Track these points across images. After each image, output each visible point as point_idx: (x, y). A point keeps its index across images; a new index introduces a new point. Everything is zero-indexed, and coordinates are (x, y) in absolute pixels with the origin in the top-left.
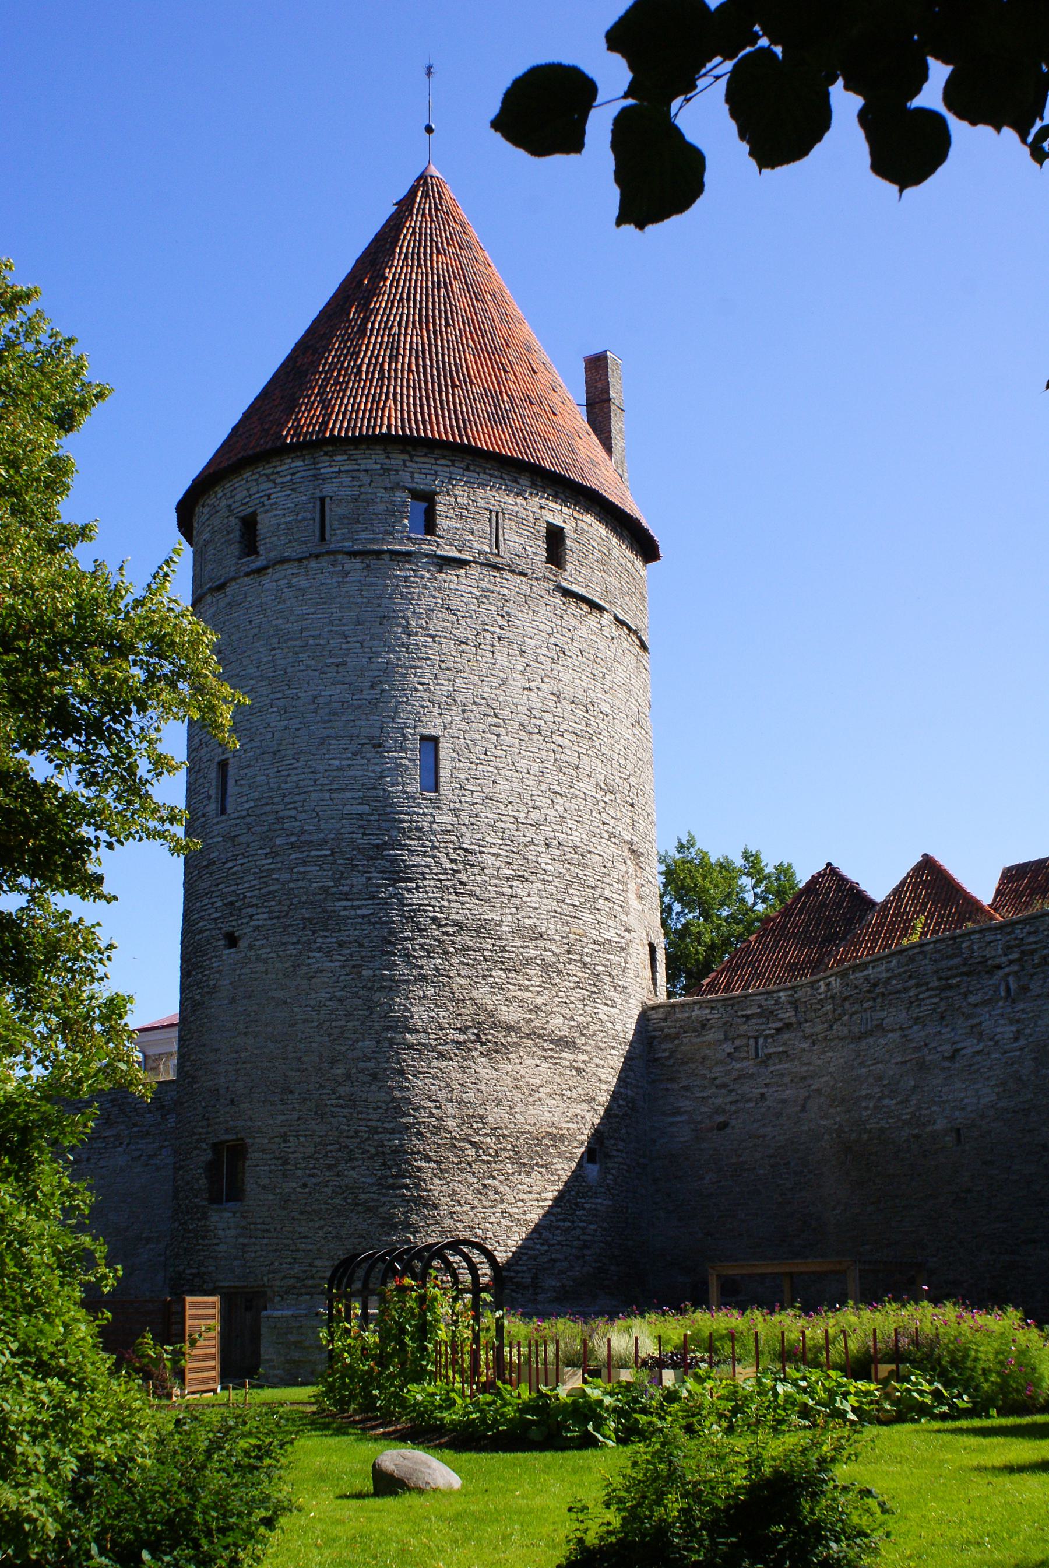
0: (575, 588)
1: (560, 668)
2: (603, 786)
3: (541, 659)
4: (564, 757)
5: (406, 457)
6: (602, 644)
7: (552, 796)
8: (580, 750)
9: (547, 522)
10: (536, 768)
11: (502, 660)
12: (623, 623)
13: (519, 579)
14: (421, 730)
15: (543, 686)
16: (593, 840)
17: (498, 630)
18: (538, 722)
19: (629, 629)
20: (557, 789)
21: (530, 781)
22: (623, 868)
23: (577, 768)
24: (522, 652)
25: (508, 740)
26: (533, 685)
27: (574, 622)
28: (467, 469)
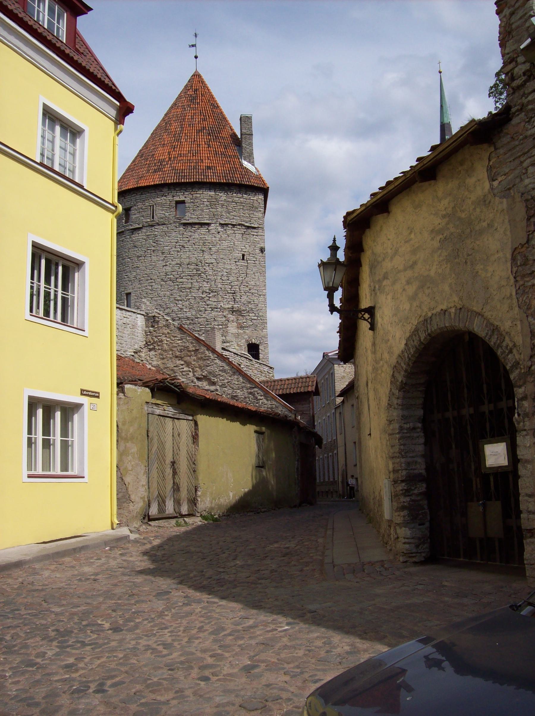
0: (191, 221)
1: (181, 253)
2: (207, 291)
3: (172, 253)
4: (183, 286)
5: (123, 198)
6: (209, 238)
7: (176, 302)
8: (192, 281)
9: (176, 201)
10: (168, 293)
11: (154, 258)
12: (227, 225)
13: (161, 227)
14: (126, 292)
15: (173, 263)
16: (200, 313)
17: (153, 248)
18: (170, 277)
19: (234, 225)
20: (179, 298)
21: (166, 299)
22: (224, 319)
23: (191, 288)
24: (163, 253)
25: (156, 286)
26: (167, 263)
27: (190, 234)
28: (142, 194)
